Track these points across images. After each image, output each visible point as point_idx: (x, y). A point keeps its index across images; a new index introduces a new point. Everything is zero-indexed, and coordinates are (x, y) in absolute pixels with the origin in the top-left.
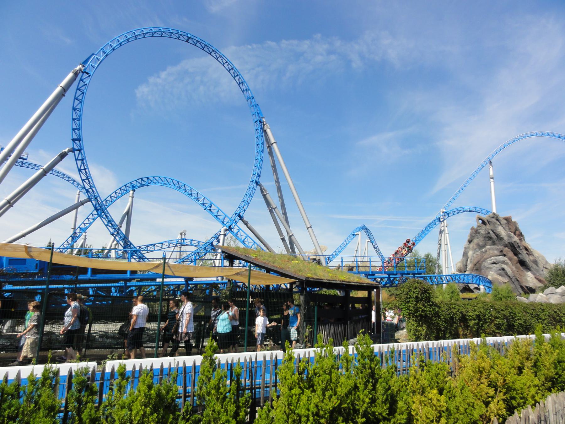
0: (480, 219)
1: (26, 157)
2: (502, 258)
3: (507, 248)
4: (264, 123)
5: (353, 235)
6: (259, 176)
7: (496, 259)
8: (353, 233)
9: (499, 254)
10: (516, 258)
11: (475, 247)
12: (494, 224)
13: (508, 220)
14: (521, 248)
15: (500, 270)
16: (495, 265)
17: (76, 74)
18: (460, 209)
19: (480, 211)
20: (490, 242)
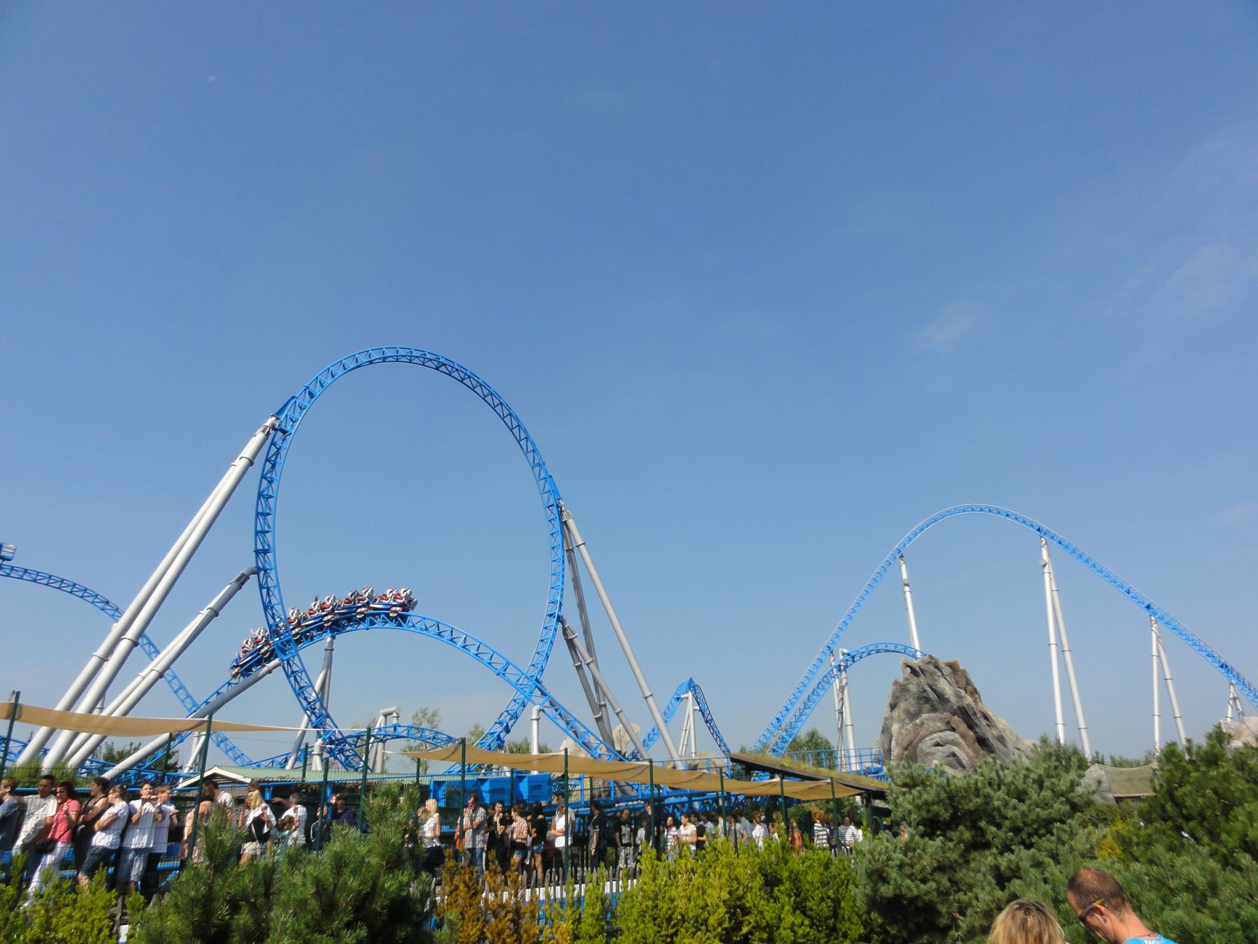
0: (908, 666)
2: (949, 735)
3: (956, 717)
4: (563, 509)
5: (678, 699)
7: (940, 737)
8: (676, 696)
9: (944, 728)
10: (972, 733)
11: (903, 716)
12: (932, 674)
13: (953, 667)
14: (979, 715)
15: (948, 756)
16: (939, 748)
18: (871, 648)
19: (902, 651)
20: (927, 706)
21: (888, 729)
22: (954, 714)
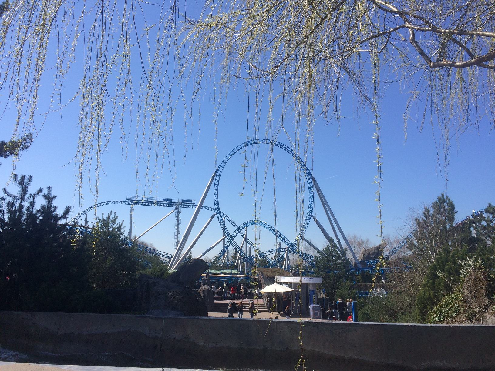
1: (194, 203)
6: (312, 211)
17: (213, 178)
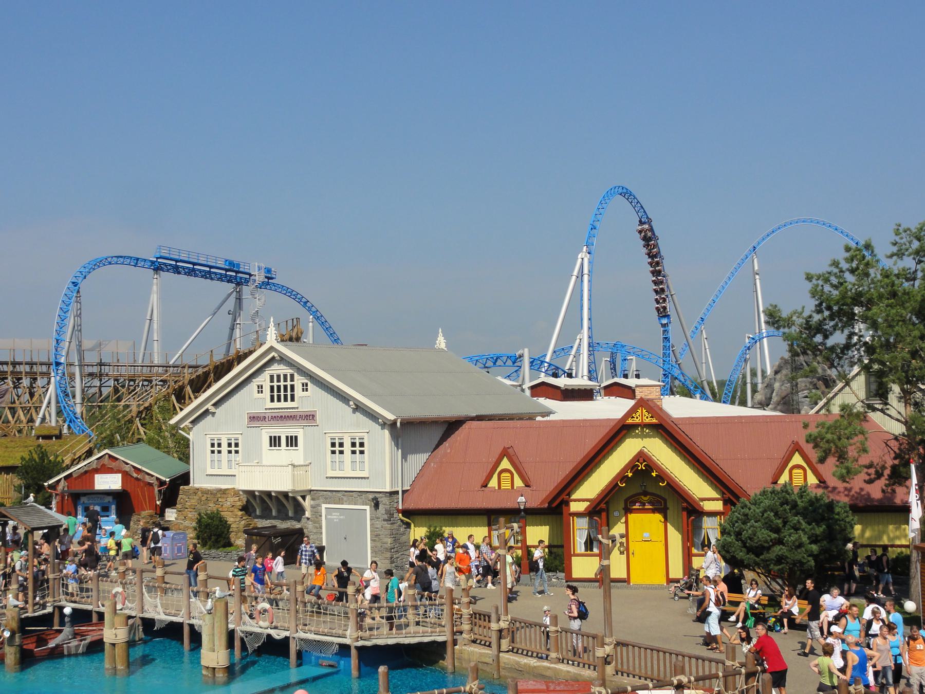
11: (783, 378)
21: (771, 385)
22: (819, 379)
